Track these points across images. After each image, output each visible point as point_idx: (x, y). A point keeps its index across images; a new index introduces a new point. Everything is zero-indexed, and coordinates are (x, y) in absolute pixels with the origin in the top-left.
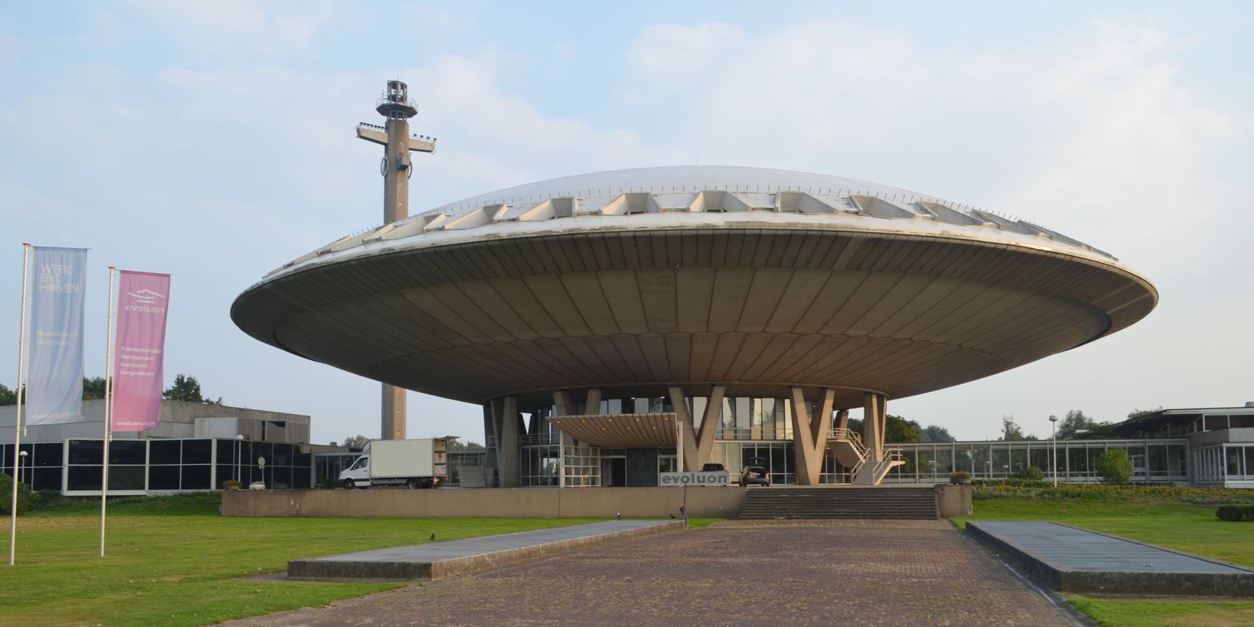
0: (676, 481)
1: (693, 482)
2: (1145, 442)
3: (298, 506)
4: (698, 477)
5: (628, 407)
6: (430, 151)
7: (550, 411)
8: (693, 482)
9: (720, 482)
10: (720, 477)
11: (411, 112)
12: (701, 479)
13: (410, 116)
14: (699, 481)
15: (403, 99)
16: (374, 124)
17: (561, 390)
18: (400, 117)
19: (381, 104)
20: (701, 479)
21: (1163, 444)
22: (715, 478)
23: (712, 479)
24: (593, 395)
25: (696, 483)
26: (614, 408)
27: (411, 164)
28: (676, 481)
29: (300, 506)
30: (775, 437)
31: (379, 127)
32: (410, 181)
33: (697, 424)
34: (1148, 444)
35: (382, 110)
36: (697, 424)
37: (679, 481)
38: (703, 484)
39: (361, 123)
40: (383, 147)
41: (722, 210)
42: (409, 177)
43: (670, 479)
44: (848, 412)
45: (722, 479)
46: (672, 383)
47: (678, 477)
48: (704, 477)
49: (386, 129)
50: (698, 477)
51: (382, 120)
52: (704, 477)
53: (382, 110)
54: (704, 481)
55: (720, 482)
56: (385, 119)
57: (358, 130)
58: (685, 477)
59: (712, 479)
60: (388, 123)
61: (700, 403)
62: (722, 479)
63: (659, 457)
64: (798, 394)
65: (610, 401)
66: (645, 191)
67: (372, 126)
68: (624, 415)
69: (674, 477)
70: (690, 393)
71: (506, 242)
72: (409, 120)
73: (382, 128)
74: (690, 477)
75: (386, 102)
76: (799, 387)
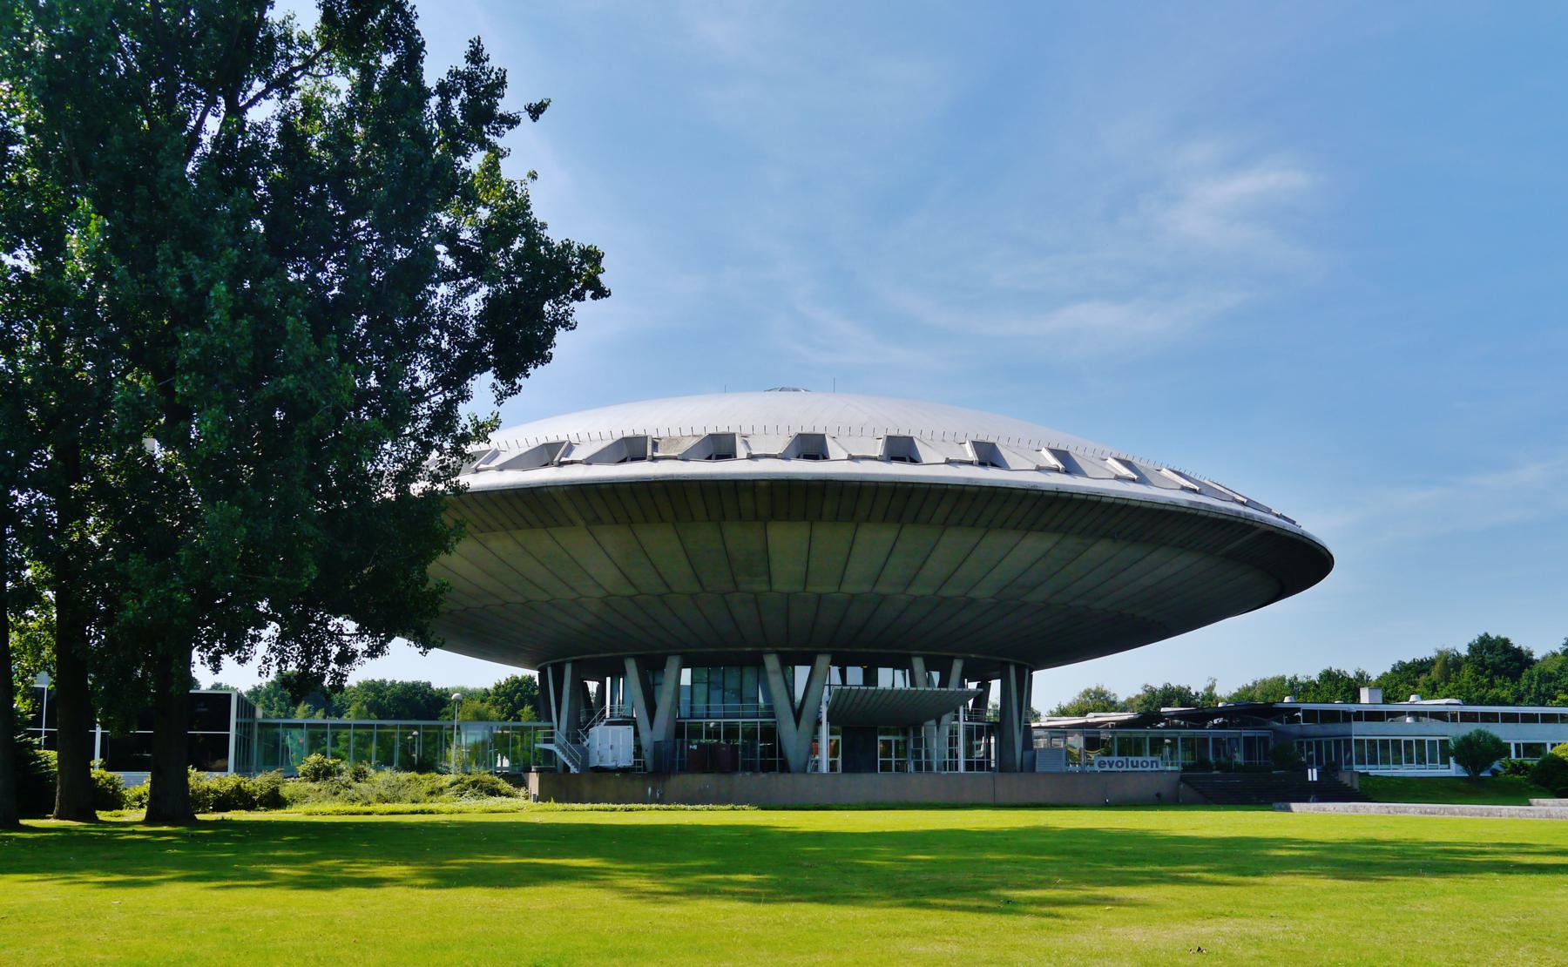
0: (1111, 766)
4: (1132, 762)
7: (621, 679)
9: (1152, 767)
10: (1152, 762)
14: (1133, 766)
17: (777, 652)
22: (1147, 763)
23: (1120, 764)
25: (1130, 769)
28: (1111, 766)
33: (799, 695)
36: (799, 695)
37: (1114, 766)
38: (1136, 769)
45: (1155, 764)
46: (917, 652)
48: (1137, 762)
50: (1132, 762)
52: (1137, 762)
54: (1137, 767)
55: (1152, 767)
59: (1120, 764)
61: (802, 673)
62: (1155, 764)
63: (880, 738)
66: (991, 440)
70: (788, 662)
74: (1125, 761)
76: (676, 654)
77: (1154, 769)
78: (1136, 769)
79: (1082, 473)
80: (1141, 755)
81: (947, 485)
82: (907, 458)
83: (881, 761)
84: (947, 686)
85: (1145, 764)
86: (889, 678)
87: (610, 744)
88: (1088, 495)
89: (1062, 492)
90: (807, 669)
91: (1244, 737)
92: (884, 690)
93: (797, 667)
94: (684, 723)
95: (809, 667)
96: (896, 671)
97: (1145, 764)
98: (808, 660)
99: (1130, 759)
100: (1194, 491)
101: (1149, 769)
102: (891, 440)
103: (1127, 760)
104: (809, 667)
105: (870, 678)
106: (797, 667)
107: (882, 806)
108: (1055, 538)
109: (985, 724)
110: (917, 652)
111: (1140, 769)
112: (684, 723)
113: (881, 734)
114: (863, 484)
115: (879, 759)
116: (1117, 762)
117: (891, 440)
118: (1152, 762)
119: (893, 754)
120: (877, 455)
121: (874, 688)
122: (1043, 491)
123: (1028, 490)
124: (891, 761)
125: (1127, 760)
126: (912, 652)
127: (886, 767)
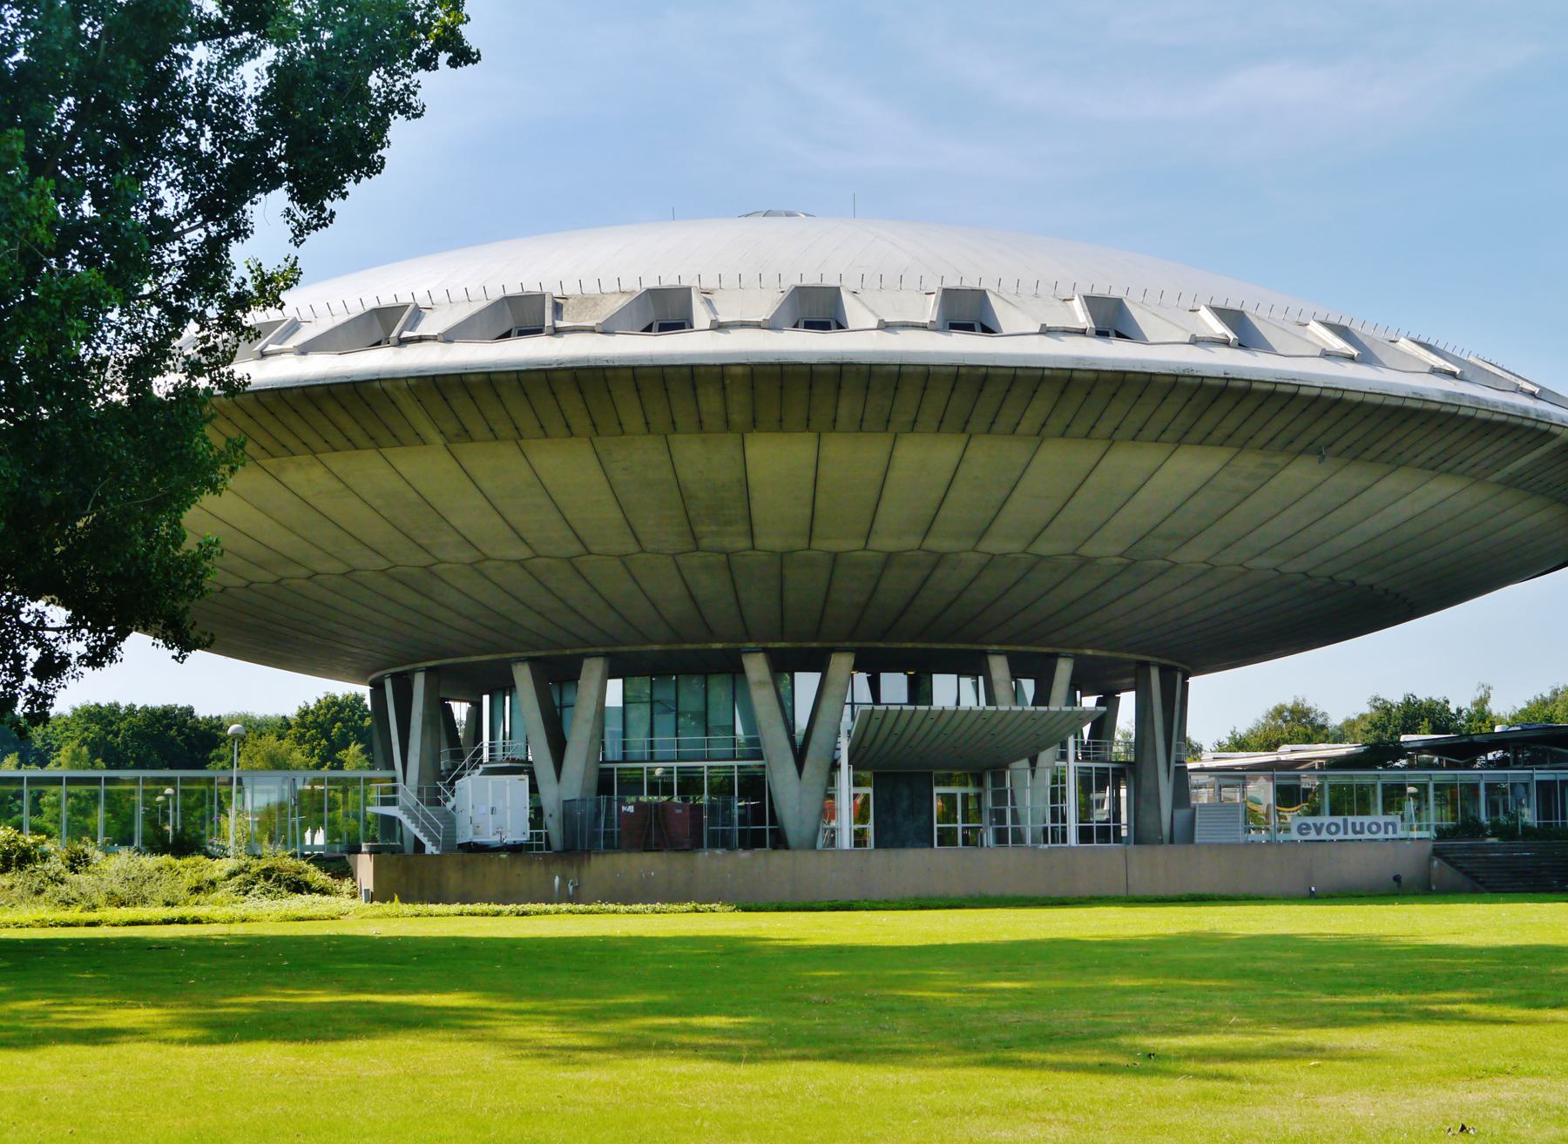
0: (1319, 832)
1: (1346, 833)
2: (1532, 775)
3: (571, 888)
7: (507, 698)
8: (1346, 833)
9: (1386, 832)
10: (1386, 824)
12: (1358, 828)
14: (1355, 832)
17: (765, 650)
20: (1358, 828)
21: (1552, 778)
22: (1378, 826)
25: (1351, 836)
28: (1319, 832)
29: (575, 888)
33: (802, 721)
34: (1536, 778)
36: (802, 721)
38: (1359, 836)
41: (977, 326)
43: (1308, 827)
45: (1390, 828)
46: (995, 648)
47: (1322, 824)
48: (1362, 824)
52: (1362, 824)
54: (1362, 832)
55: (1386, 832)
59: (1333, 829)
61: (806, 684)
62: (1390, 828)
63: (937, 790)
66: (1115, 294)
69: (1315, 825)
70: (784, 665)
71: (1109, 375)
74: (1341, 824)
77: (1390, 835)
78: (1359, 836)
79: (1266, 347)
80: (1367, 813)
81: (1044, 369)
82: (977, 326)
83: (939, 829)
84: (1046, 703)
85: (1374, 828)
86: (949, 691)
87: (491, 805)
88: (1276, 383)
89: (1234, 379)
90: (815, 677)
91: (1537, 782)
92: (943, 710)
93: (798, 675)
94: (612, 769)
95: (818, 675)
96: (961, 679)
97: (1374, 828)
98: (818, 662)
99: (1351, 819)
100: (1453, 375)
101: (1381, 835)
102: (950, 297)
103: (1345, 821)
104: (818, 675)
105: (919, 692)
106: (798, 675)
107: (941, 903)
108: (1224, 454)
109: (1110, 766)
110: (995, 648)
111: (1367, 835)
112: (612, 769)
113: (938, 784)
114: (903, 369)
115: (936, 826)
116: (1329, 825)
117: (950, 297)
118: (1386, 824)
119: (959, 817)
120: (927, 321)
121: (926, 708)
122: (1203, 377)
123: (1177, 376)
124: (956, 829)
125: (1345, 821)
127: (947, 838)
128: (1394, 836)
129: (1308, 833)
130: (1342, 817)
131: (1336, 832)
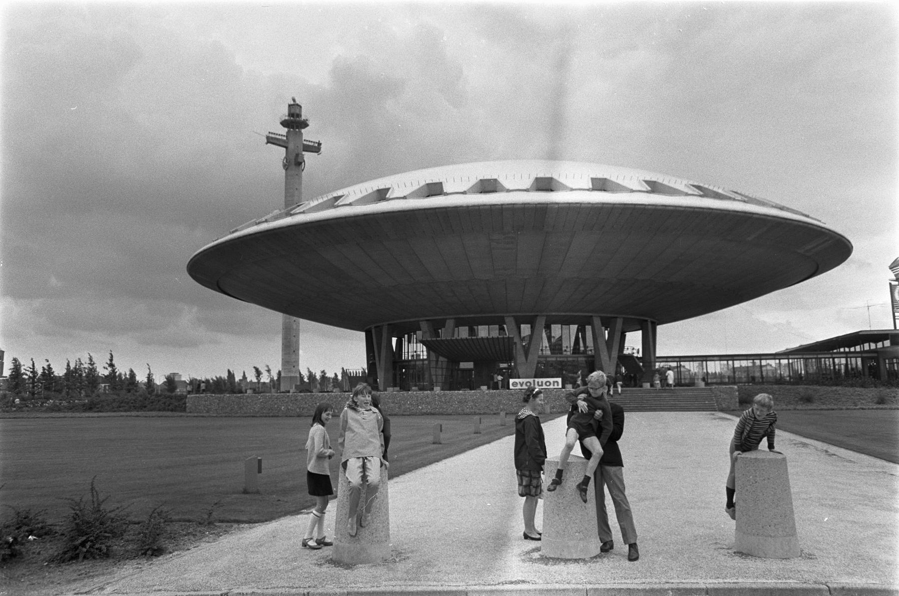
0: (521, 385)
4: (538, 382)
5: (472, 332)
6: (317, 152)
9: (554, 385)
10: (554, 382)
11: (305, 124)
12: (540, 384)
13: (304, 128)
14: (538, 385)
15: (299, 115)
16: (278, 133)
18: (297, 128)
19: (283, 119)
20: (540, 384)
24: (450, 323)
26: (463, 333)
27: (304, 161)
28: (521, 385)
30: (856, 359)
31: (282, 135)
32: (303, 173)
35: (284, 124)
39: (269, 133)
40: (285, 149)
42: (303, 170)
43: (517, 383)
44: (625, 335)
46: (508, 315)
47: (523, 382)
48: (542, 382)
49: (287, 137)
50: (538, 382)
51: (284, 131)
52: (542, 382)
53: (284, 124)
55: (554, 385)
56: (286, 129)
57: (268, 138)
58: (528, 382)
60: (287, 133)
64: (597, 322)
65: (459, 327)
67: (277, 134)
68: (470, 338)
69: (520, 383)
72: (303, 131)
73: (284, 136)
75: (287, 118)
77: (556, 387)
79: (564, 188)
86: (483, 332)
101: (552, 387)
102: (594, 180)
103: (534, 381)
105: (472, 332)
111: (544, 387)
117: (594, 180)
125: (534, 381)
126: (505, 315)
128: (558, 387)
129: (516, 386)
130: (533, 379)
131: (550, 385)
